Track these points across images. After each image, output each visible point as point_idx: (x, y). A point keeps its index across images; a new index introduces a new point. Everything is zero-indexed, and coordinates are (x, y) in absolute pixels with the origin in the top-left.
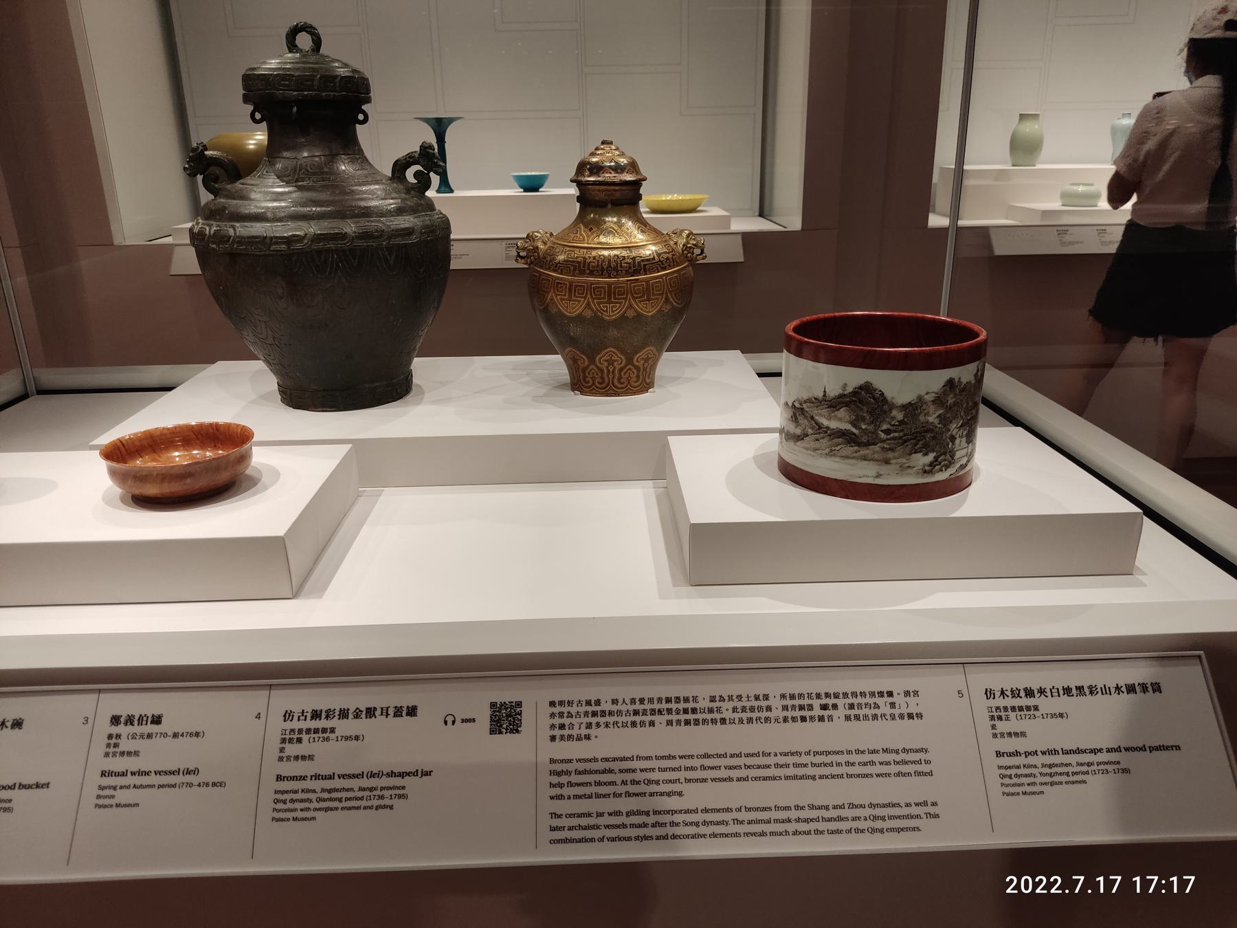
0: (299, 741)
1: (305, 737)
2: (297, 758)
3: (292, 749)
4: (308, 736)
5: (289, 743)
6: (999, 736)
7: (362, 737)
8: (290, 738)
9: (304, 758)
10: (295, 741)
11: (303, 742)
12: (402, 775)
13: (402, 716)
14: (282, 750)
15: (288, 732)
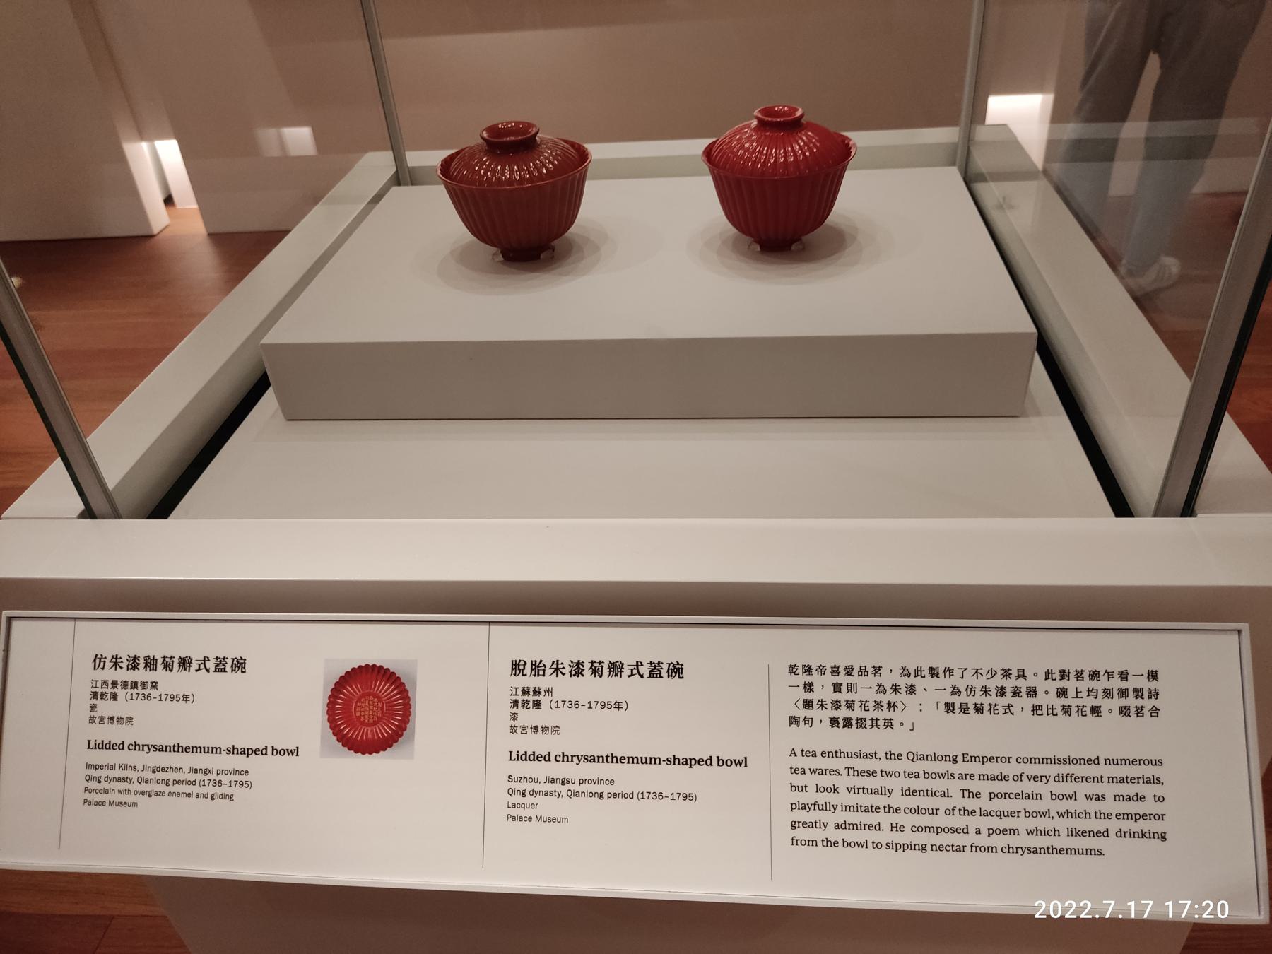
0: (114, 697)
1: (120, 692)
2: (112, 718)
3: (106, 708)
4: (124, 691)
5: (102, 698)
6: (519, 730)
7: (191, 696)
8: (102, 693)
9: (120, 720)
10: (108, 697)
11: (118, 698)
12: (246, 752)
13: (225, 671)
14: (93, 708)
15: (99, 684)
